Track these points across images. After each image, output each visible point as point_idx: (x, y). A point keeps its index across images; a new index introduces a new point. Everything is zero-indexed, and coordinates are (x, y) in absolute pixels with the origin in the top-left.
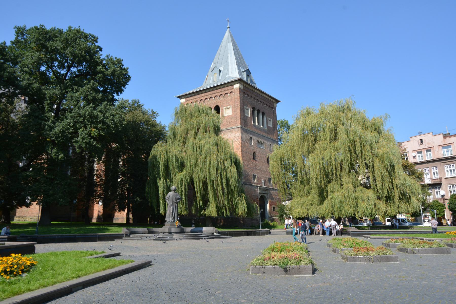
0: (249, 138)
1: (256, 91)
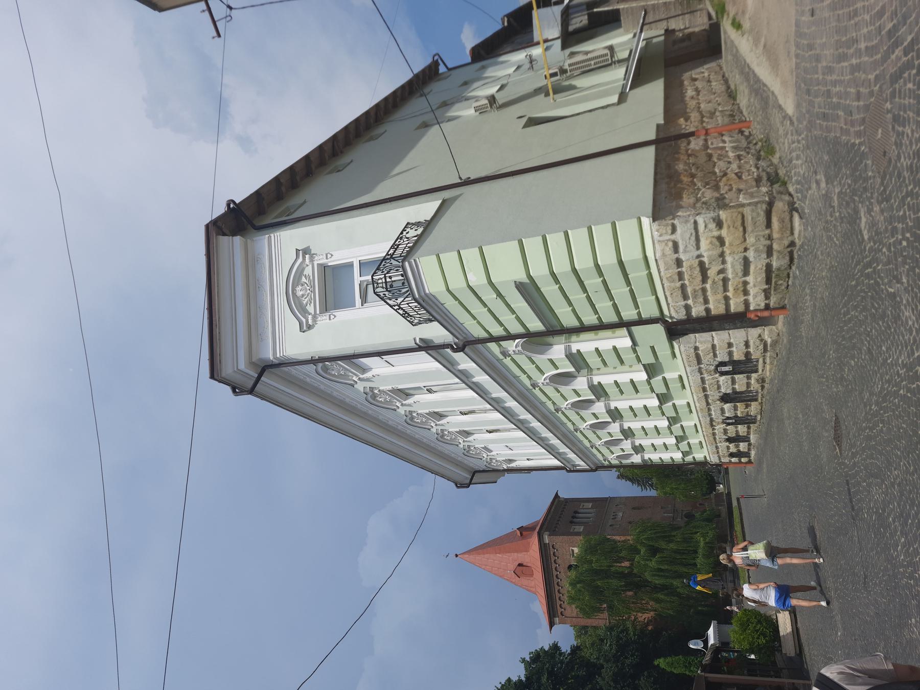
1: (548, 518)
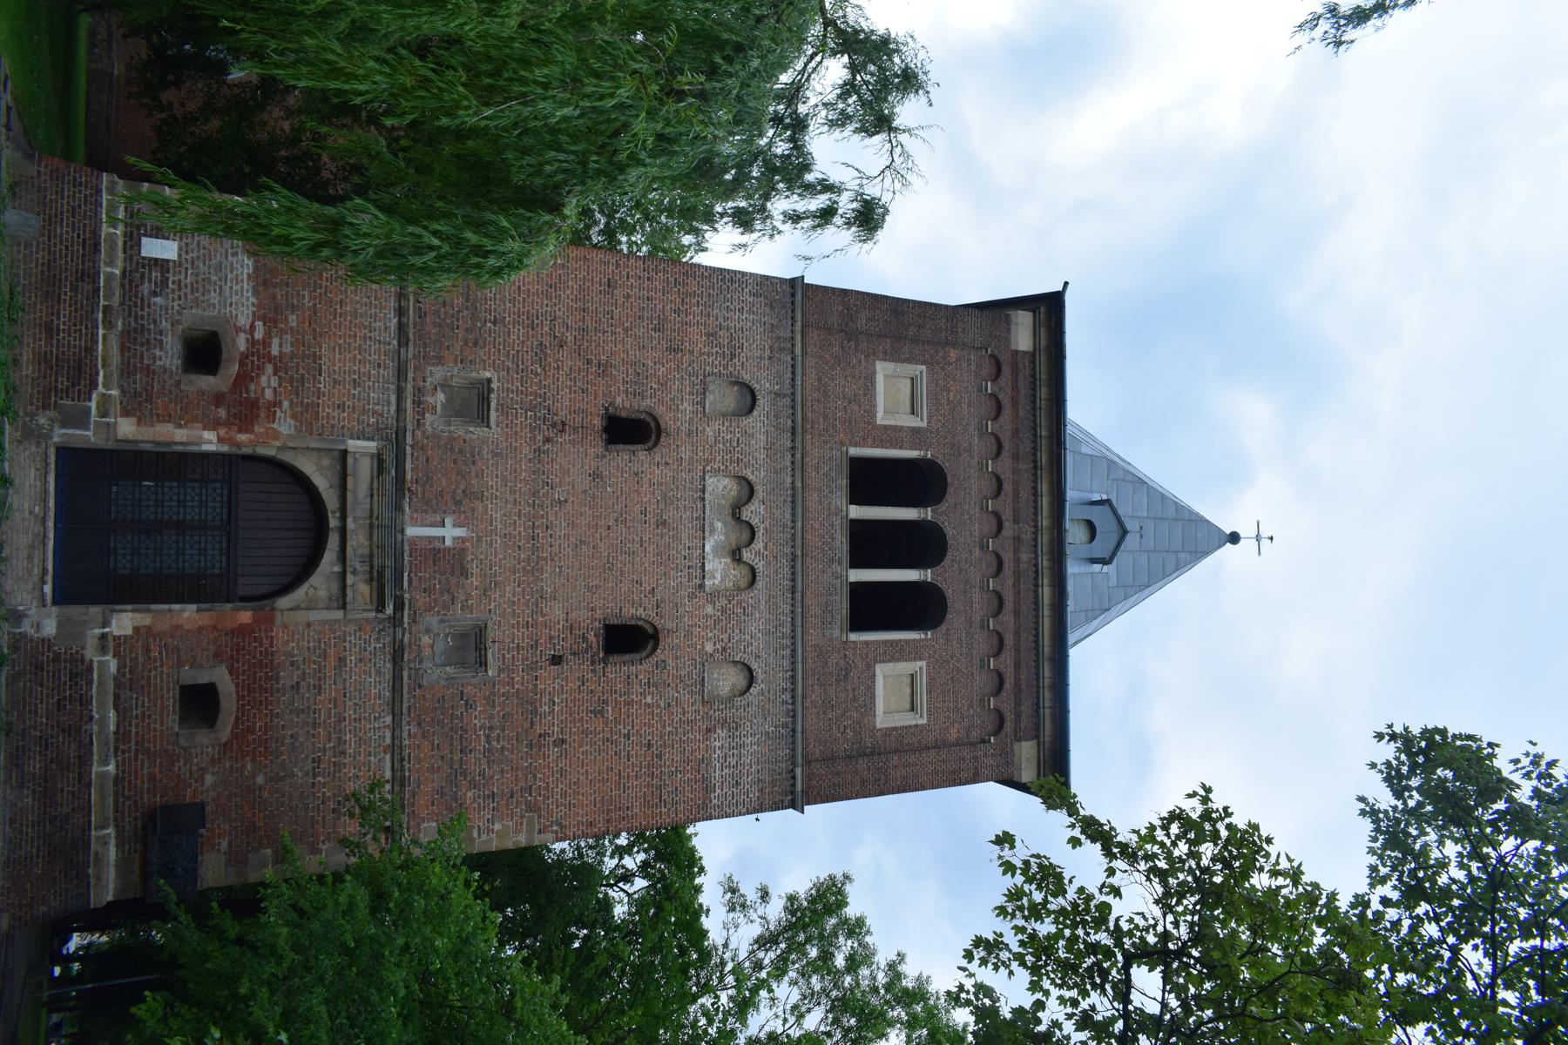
1: (1044, 488)
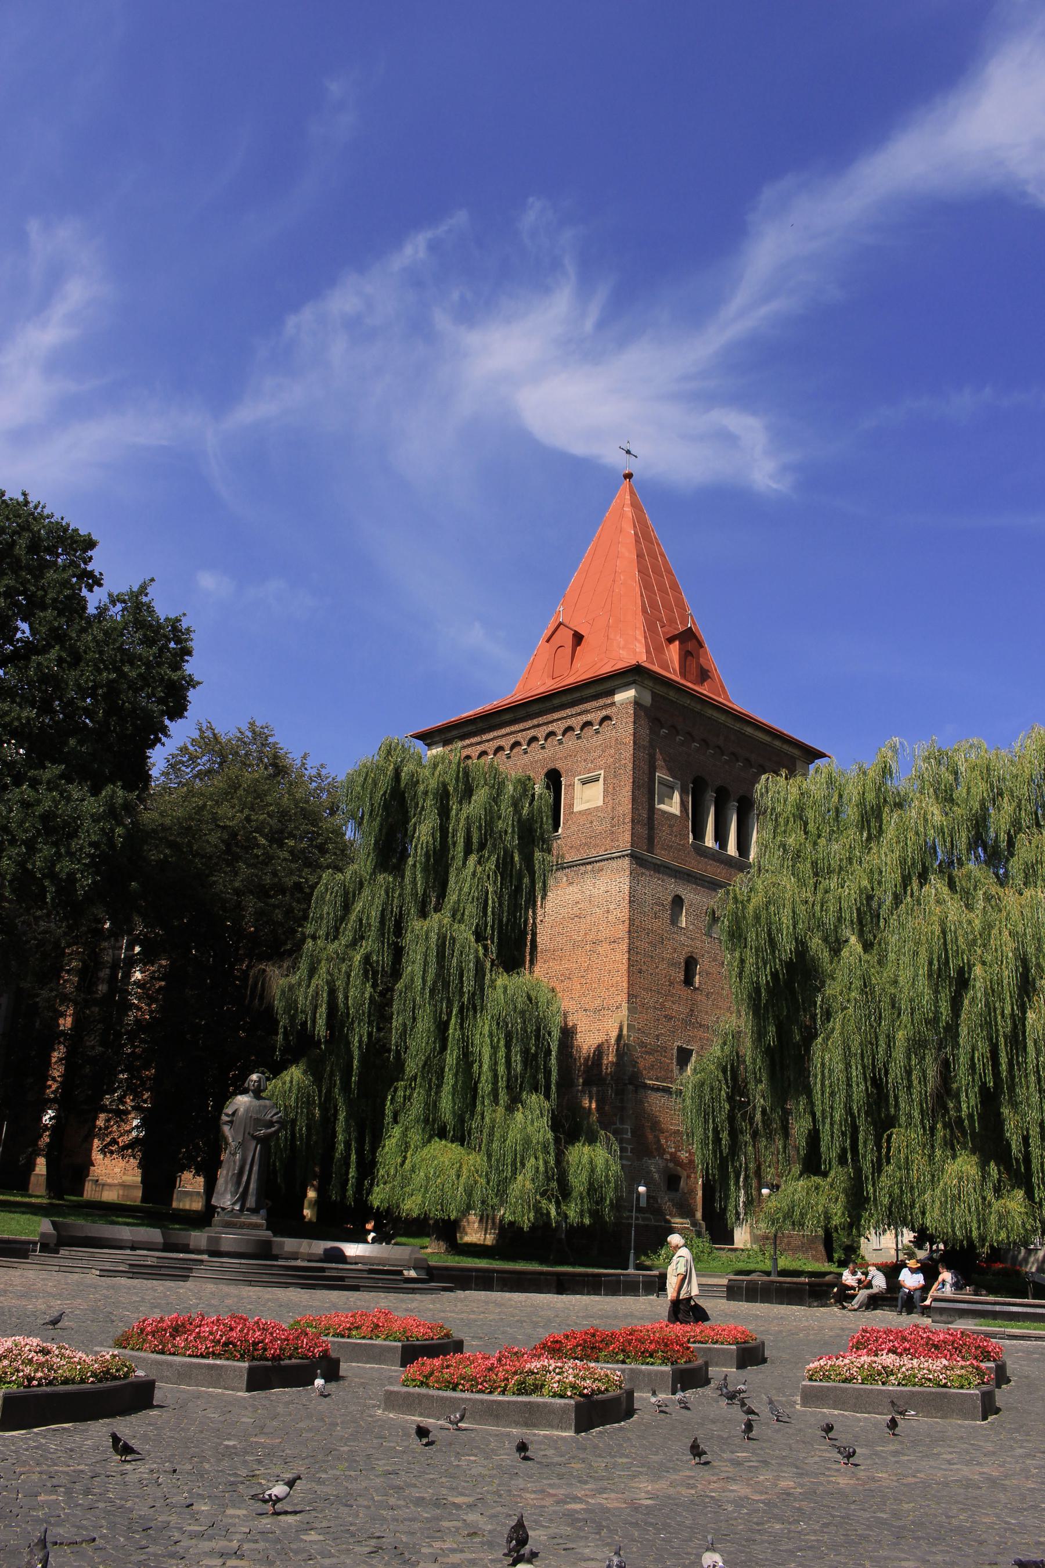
0: (670, 899)
1: (710, 712)
